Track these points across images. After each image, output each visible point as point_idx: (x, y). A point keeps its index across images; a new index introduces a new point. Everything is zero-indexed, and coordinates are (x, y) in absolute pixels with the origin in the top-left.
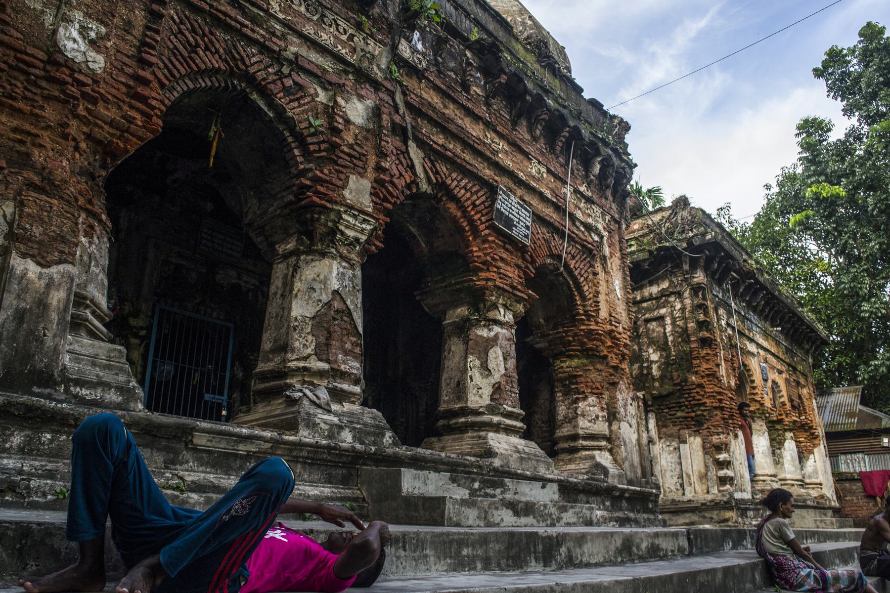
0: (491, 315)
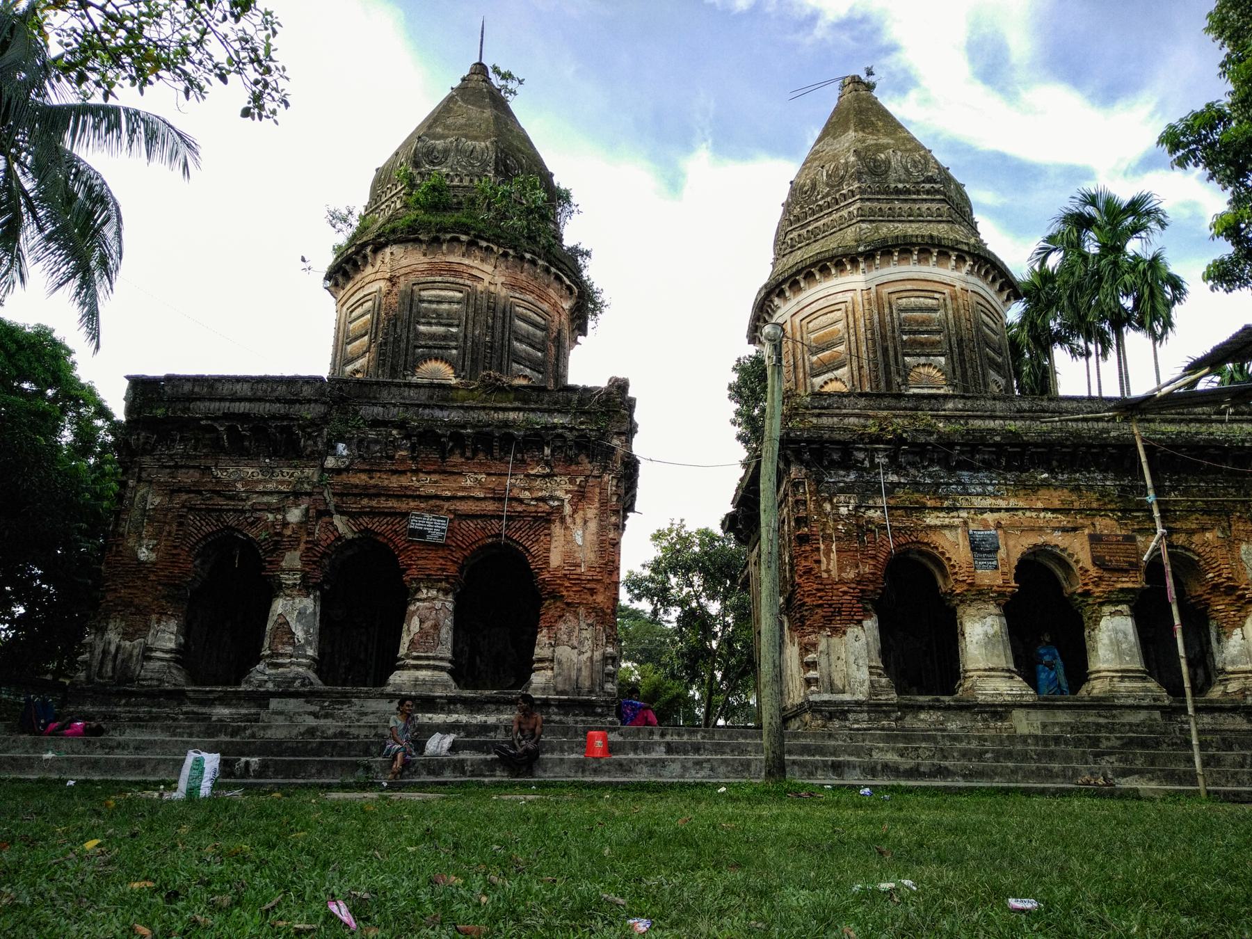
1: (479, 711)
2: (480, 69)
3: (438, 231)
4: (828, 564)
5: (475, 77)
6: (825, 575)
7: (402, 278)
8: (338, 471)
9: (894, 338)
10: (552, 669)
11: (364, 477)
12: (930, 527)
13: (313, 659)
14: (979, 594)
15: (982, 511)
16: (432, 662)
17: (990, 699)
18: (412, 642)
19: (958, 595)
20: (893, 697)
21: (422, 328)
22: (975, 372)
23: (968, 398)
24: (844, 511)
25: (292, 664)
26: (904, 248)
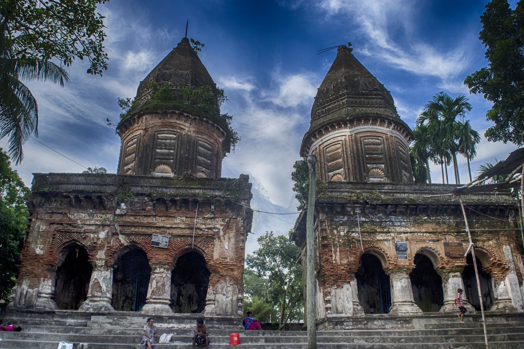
0: (155, 271)
1: (182, 323)
2: (185, 40)
3: (166, 109)
4: (336, 257)
5: (184, 44)
6: (334, 262)
7: (150, 129)
8: (122, 215)
9: (363, 156)
10: (214, 304)
11: (132, 218)
12: (378, 240)
13: (110, 298)
14: (399, 269)
15: (400, 233)
16: (161, 301)
17: (403, 315)
18: (153, 291)
19: (390, 269)
20: (363, 314)
21: (158, 151)
22: (397, 171)
23: (394, 184)
24: (342, 233)
25: (100, 300)
26: (366, 118)
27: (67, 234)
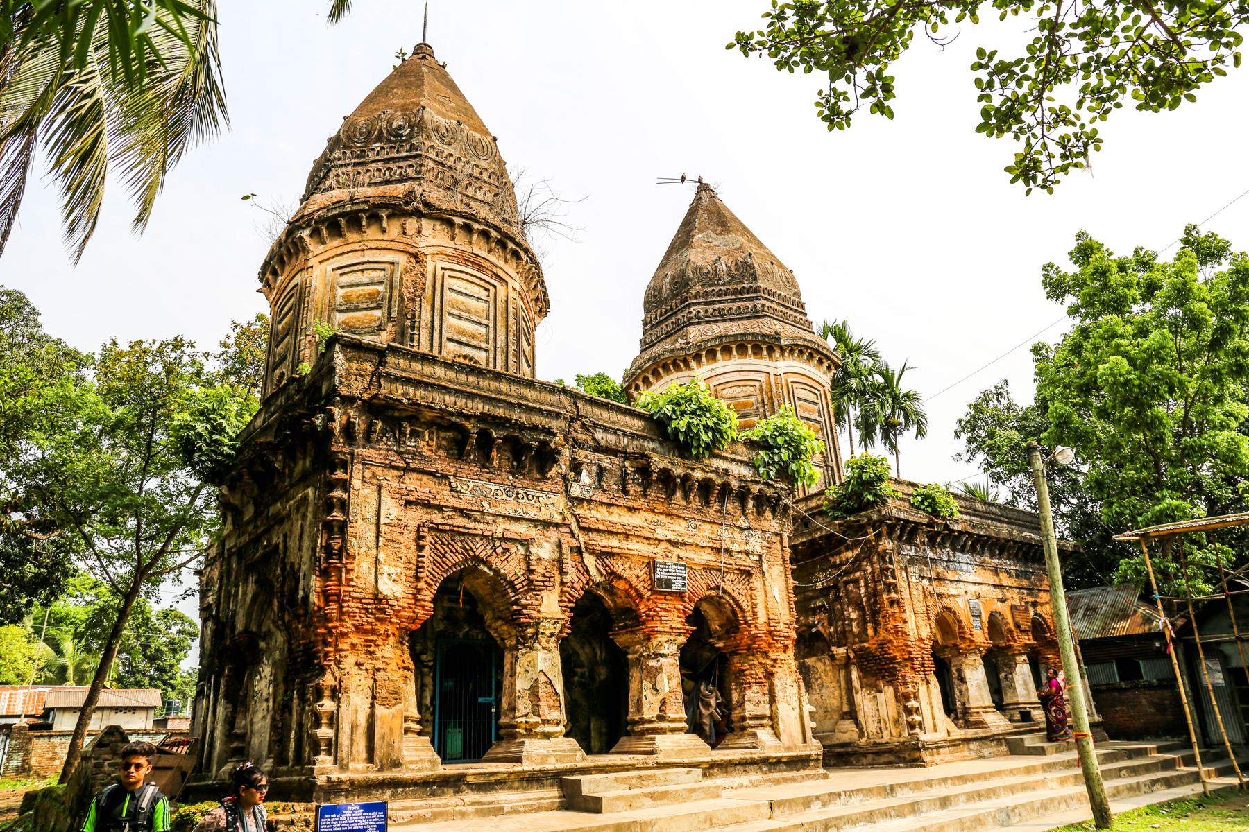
8: (580, 501)
27: (457, 538)
